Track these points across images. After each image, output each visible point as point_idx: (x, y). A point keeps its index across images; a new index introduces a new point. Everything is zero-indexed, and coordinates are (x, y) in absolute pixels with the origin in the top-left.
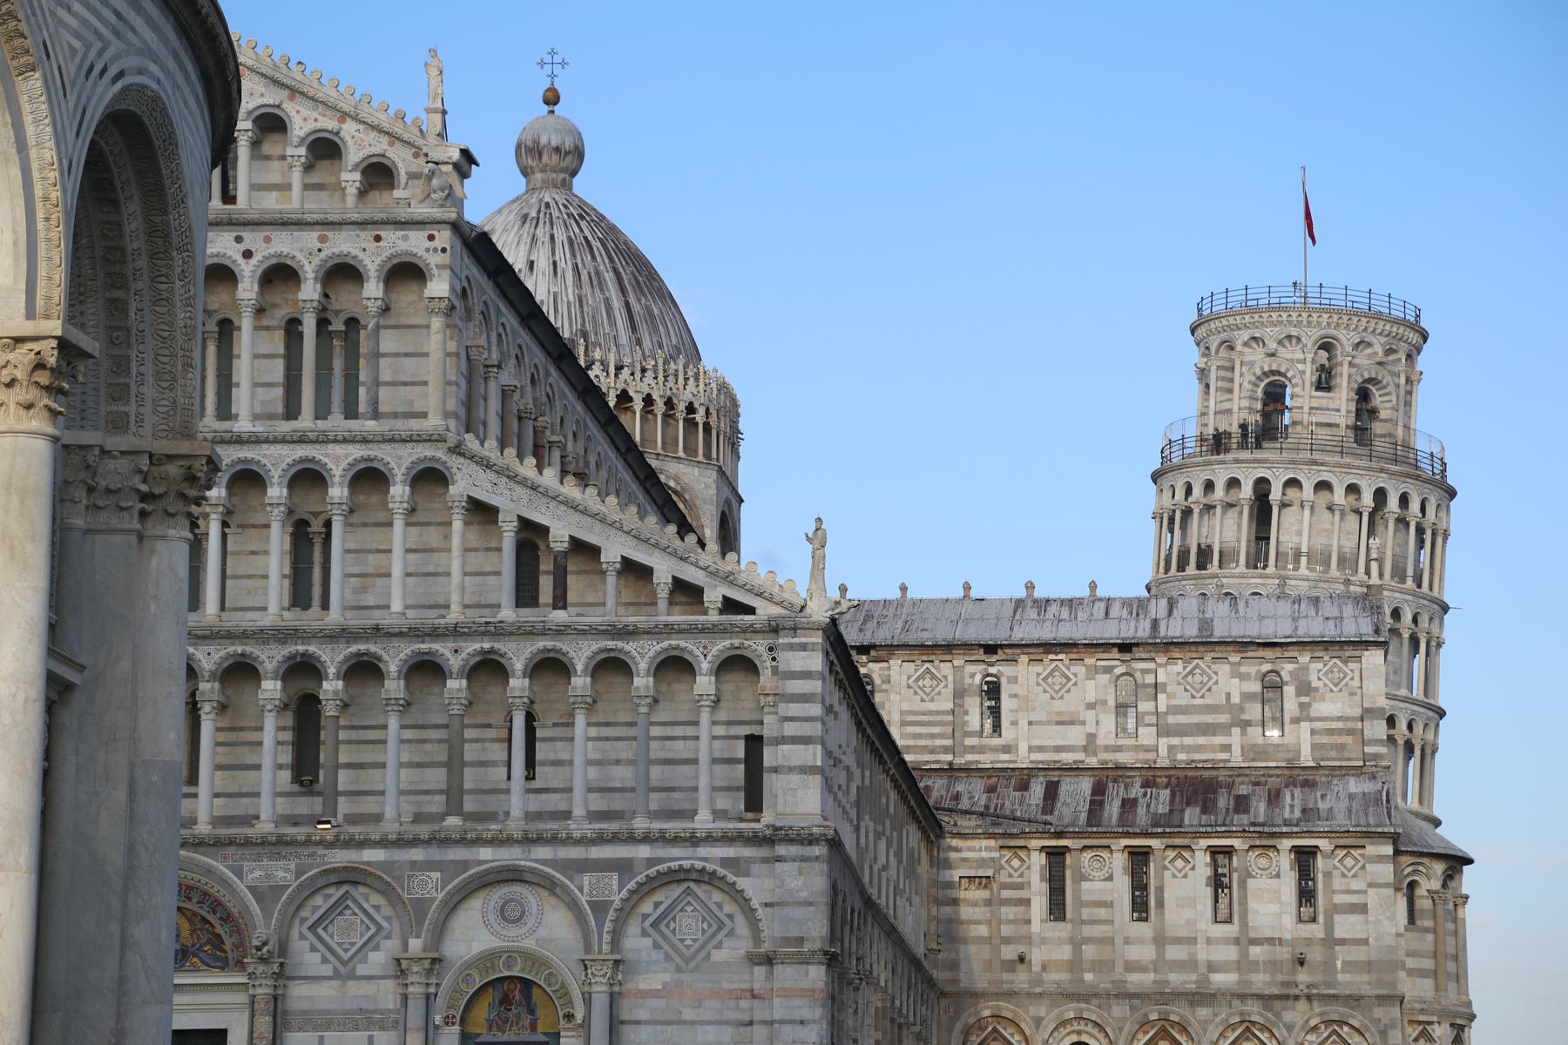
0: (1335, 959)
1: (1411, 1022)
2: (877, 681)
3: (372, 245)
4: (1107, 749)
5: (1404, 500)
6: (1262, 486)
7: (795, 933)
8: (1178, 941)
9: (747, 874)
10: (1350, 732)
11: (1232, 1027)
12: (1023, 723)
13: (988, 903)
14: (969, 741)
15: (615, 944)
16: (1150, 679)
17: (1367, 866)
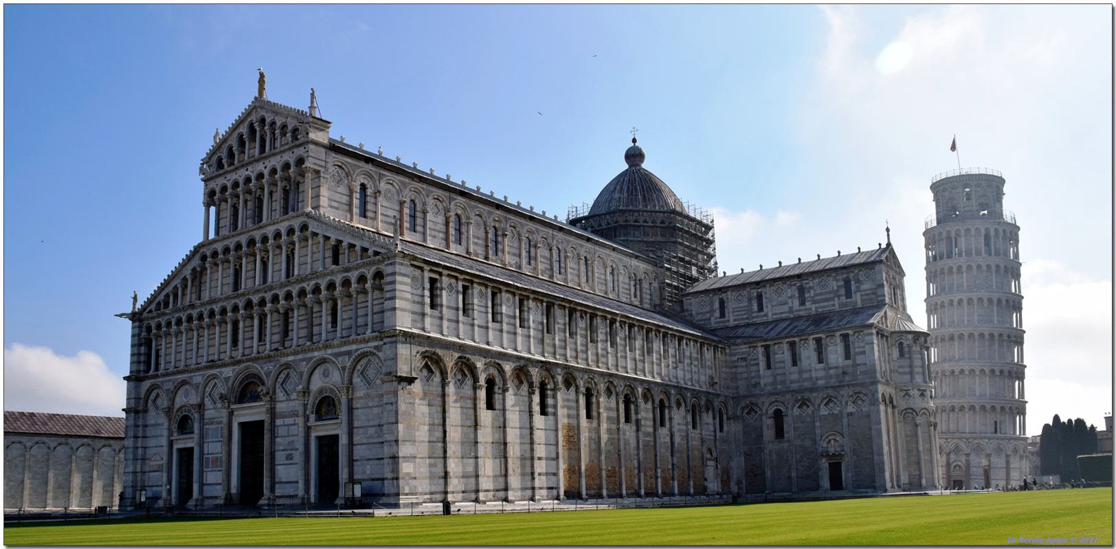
0: (857, 371)
1: (901, 390)
2: (725, 299)
3: (291, 155)
4: (797, 311)
5: (996, 231)
6: (949, 231)
7: (389, 371)
8: (806, 371)
9: (381, 351)
10: (873, 293)
11: (825, 398)
12: (769, 306)
13: (747, 366)
14: (754, 315)
15: (351, 382)
16: (808, 286)
17: (865, 338)
